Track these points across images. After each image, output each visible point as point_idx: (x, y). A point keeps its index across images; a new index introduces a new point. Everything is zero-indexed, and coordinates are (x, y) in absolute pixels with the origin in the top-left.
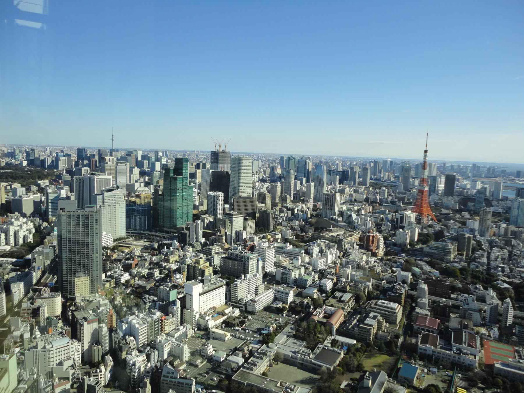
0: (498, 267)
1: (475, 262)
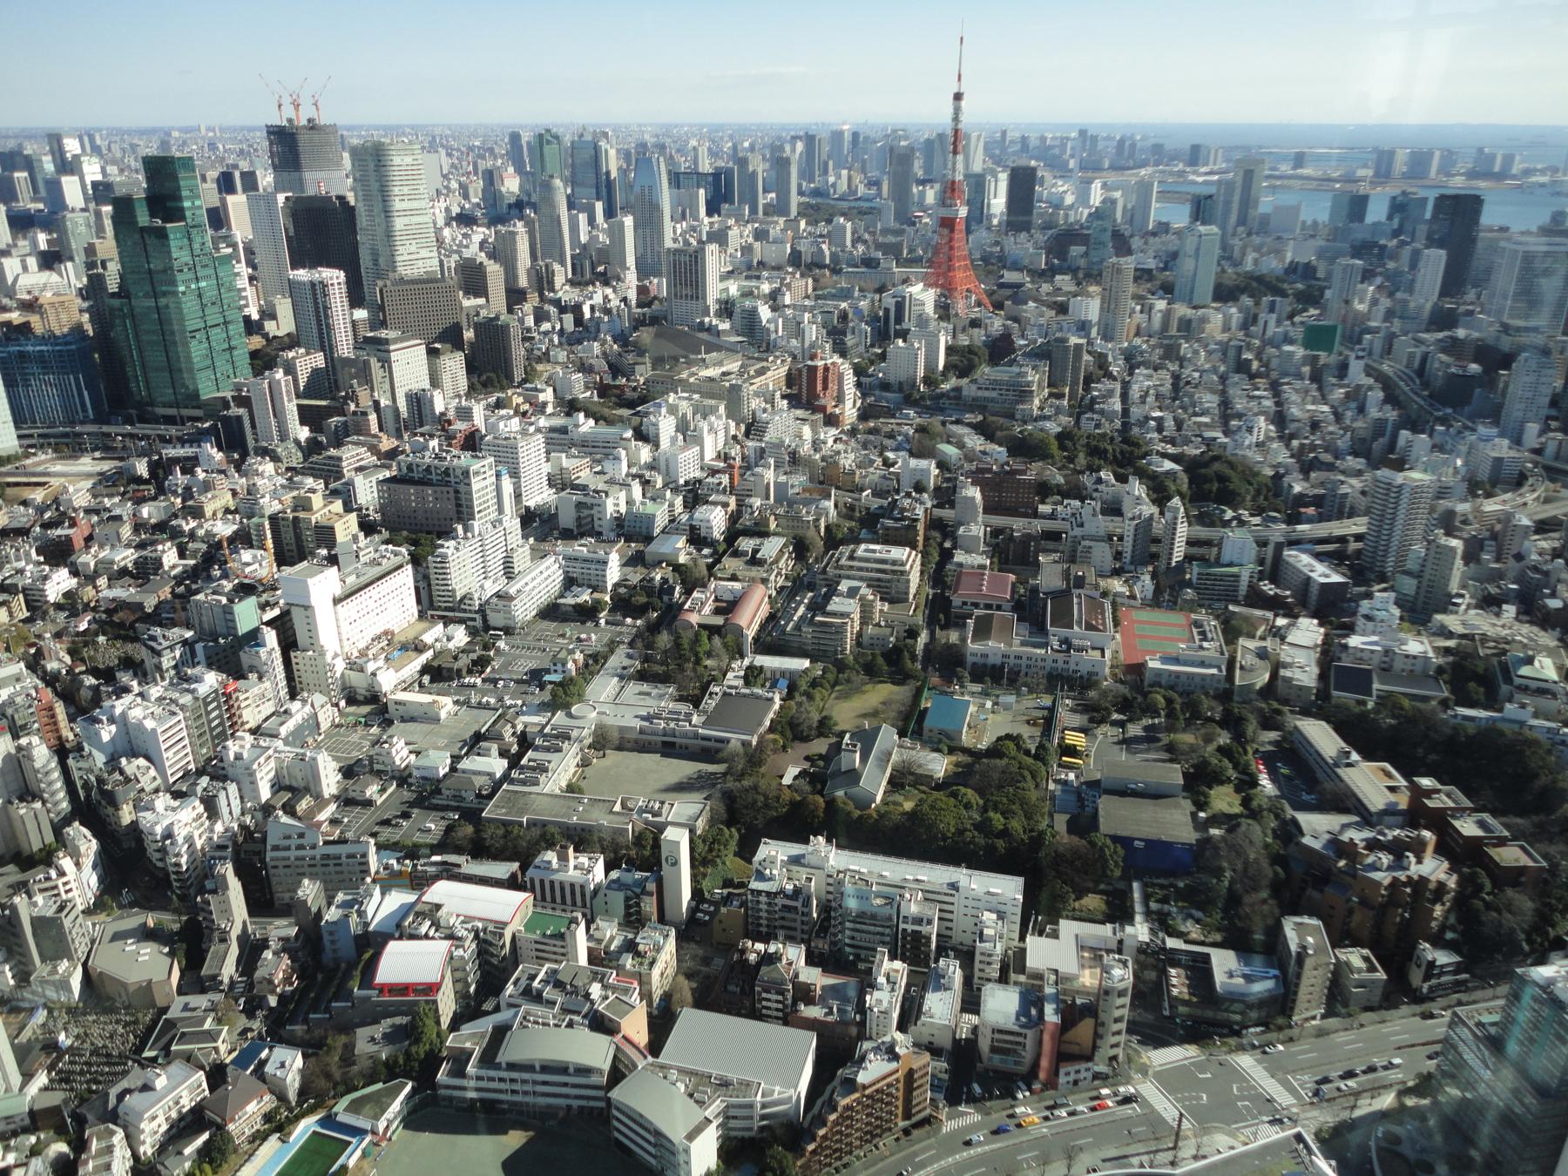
0: (1147, 418)
1: (1092, 410)
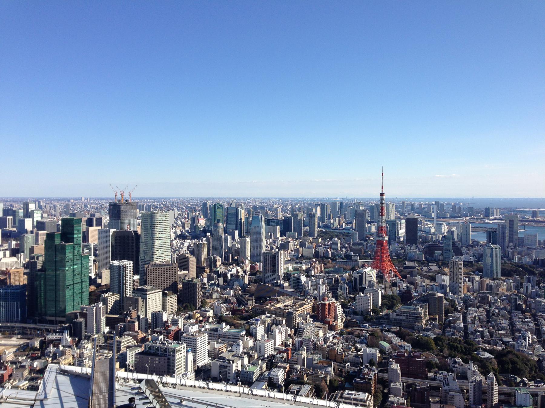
0: (476, 331)
1: (450, 327)
